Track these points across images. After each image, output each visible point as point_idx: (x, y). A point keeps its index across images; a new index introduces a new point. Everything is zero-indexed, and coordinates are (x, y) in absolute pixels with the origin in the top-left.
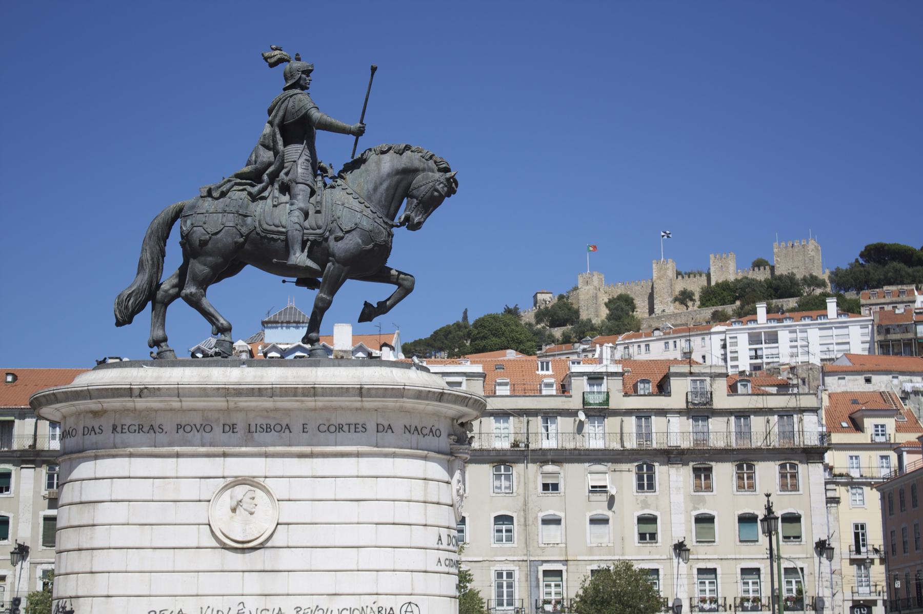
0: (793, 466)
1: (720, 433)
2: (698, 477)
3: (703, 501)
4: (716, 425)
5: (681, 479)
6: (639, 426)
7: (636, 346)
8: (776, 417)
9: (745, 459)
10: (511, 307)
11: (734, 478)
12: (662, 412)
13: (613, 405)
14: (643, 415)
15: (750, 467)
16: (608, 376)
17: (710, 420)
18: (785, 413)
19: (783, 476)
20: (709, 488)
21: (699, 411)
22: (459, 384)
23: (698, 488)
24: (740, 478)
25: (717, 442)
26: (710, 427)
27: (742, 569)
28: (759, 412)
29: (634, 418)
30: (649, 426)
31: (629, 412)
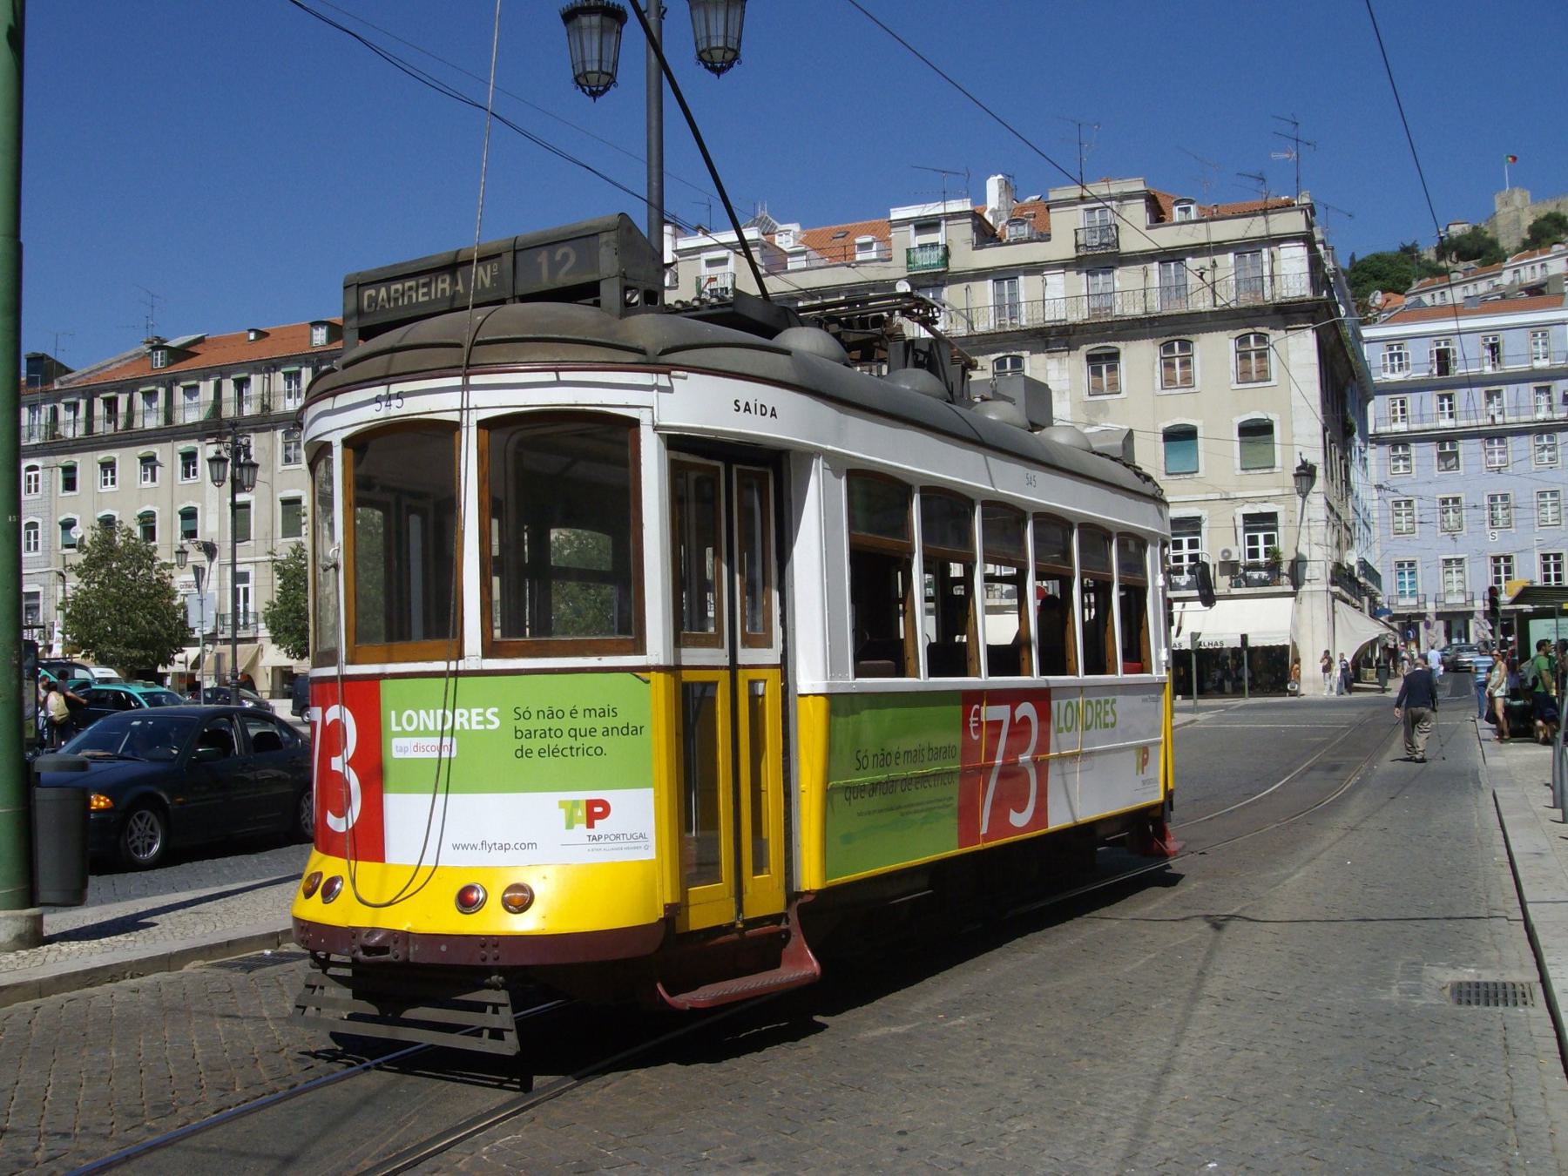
0: (1261, 338)
1: (1132, 291)
2: (1096, 372)
3: (1103, 409)
4: (1125, 279)
5: (1066, 376)
6: (999, 295)
7: (1529, 267)
8: (1231, 255)
9: (1174, 331)
10: (1408, 244)
11: (1158, 367)
12: (1035, 269)
13: (956, 264)
14: (1004, 275)
15: (1186, 345)
16: (947, 219)
17: (1117, 272)
18: (1246, 248)
19: (1244, 356)
20: (1114, 388)
21: (1098, 259)
22: (724, 261)
23: (1096, 390)
24: (1169, 365)
25: (1129, 308)
26: (1117, 284)
27: (1246, 517)
28: (1198, 250)
29: (990, 282)
30: (1013, 294)
31: (980, 275)
